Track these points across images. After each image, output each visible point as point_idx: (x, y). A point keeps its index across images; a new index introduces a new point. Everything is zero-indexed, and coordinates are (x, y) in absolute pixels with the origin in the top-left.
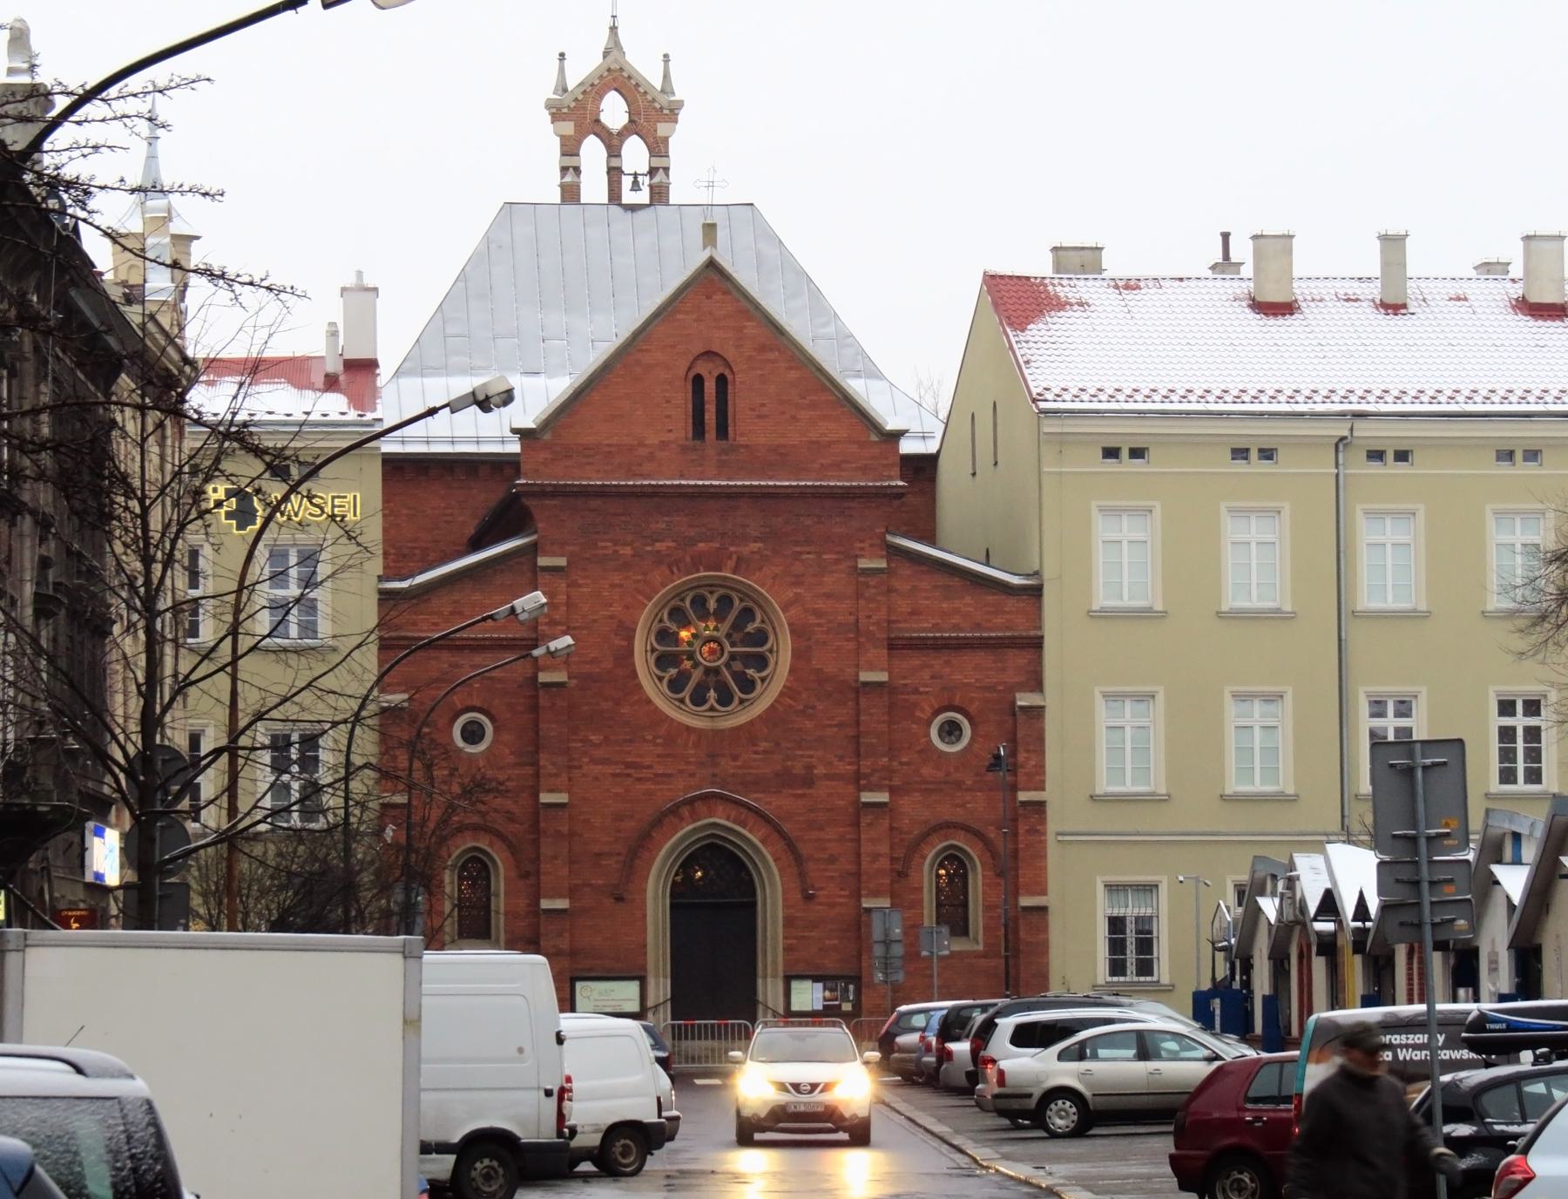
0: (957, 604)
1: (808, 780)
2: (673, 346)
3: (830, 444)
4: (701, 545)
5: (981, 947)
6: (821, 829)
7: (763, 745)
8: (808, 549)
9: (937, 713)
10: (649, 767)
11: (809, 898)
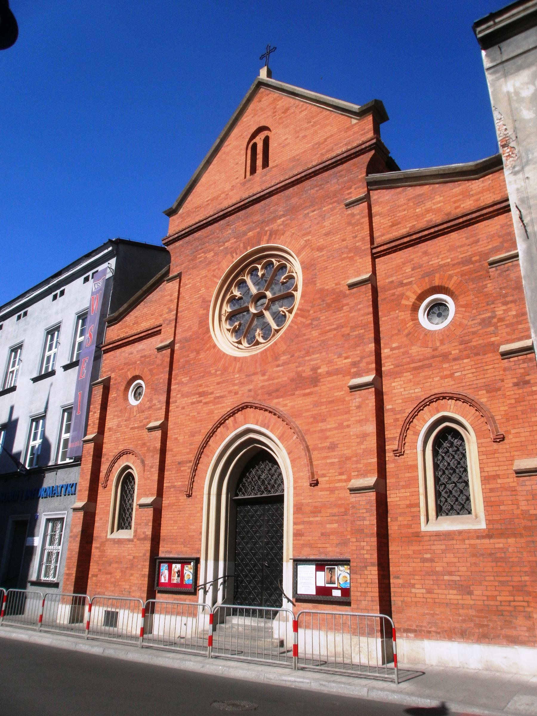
0: (428, 205)
1: (315, 380)
2: (242, 135)
3: (326, 140)
4: (250, 234)
5: (483, 525)
6: (323, 421)
7: (284, 358)
8: (313, 209)
9: (421, 298)
10: (212, 393)
11: (315, 484)
